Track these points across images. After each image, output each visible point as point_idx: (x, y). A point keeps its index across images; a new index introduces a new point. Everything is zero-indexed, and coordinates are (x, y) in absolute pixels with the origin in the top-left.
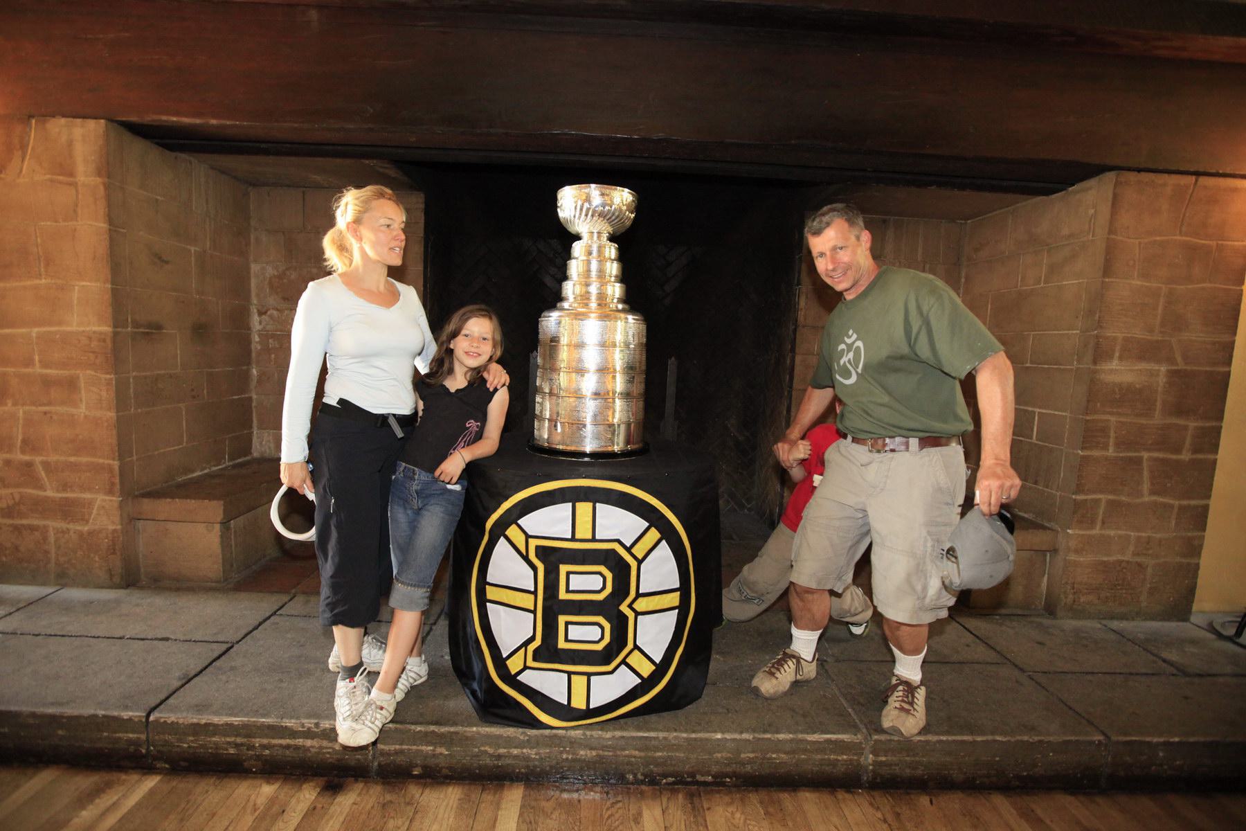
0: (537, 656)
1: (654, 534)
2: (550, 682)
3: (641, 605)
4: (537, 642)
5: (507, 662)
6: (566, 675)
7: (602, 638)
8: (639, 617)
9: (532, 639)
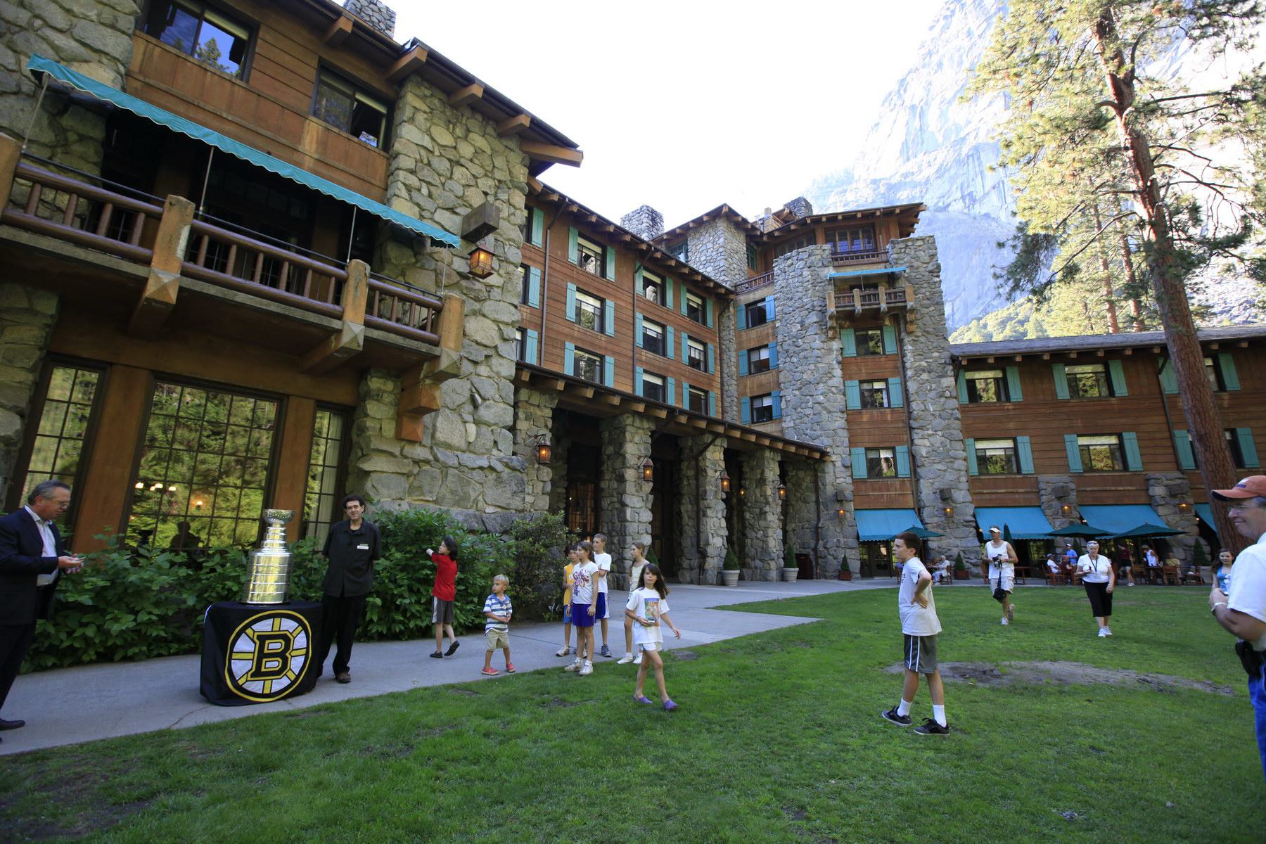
0: (252, 676)
1: (300, 628)
2: (256, 686)
3: (293, 653)
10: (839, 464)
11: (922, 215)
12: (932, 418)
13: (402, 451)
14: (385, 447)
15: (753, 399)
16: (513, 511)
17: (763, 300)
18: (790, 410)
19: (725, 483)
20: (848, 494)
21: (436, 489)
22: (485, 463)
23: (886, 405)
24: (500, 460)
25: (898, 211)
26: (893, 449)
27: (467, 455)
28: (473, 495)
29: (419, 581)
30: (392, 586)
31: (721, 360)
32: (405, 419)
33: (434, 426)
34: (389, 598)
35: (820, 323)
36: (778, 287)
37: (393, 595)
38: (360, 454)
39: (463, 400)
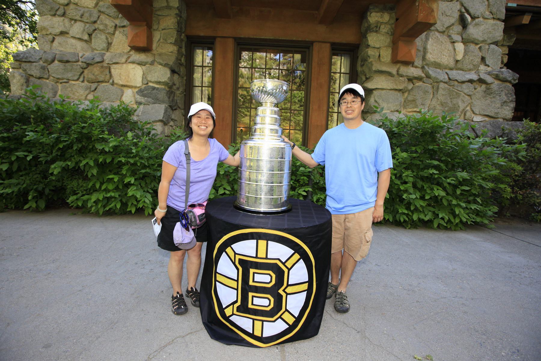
0: (238, 309)
1: (297, 256)
3: (289, 290)
4: (239, 303)
5: (225, 310)
6: (252, 320)
7: (270, 305)
8: (288, 296)
9: (236, 302)
13: (398, 71)
14: (384, 68)
16: (501, 120)
21: (428, 102)
22: (475, 77)
24: (489, 74)
27: (454, 72)
28: (462, 106)
29: (423, 179)
30: (398, 182)
32: (401, 44)
33: (425, 49)
34: (394, 191)
37: (399, 189)
38: (364, 79)
39: (452, 21)
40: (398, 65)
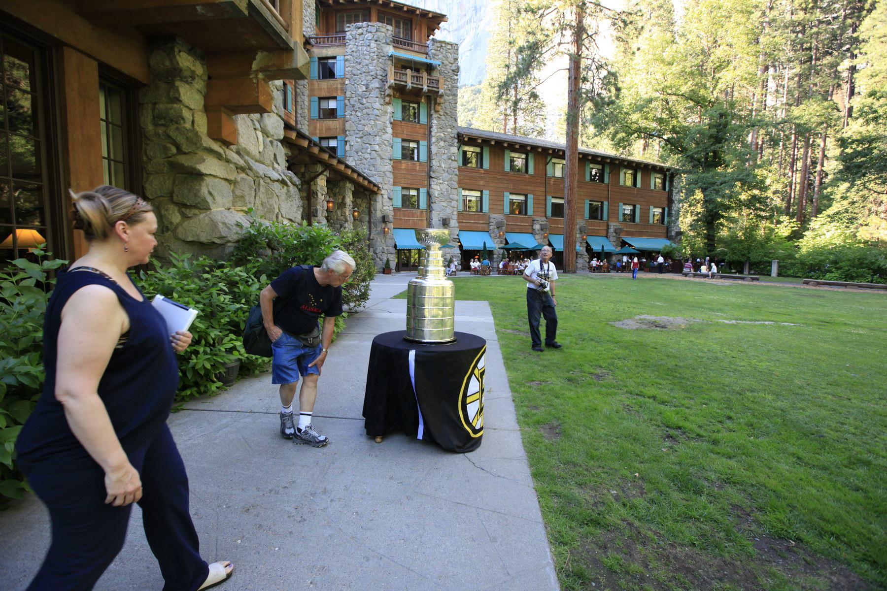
10: (385, 196)
11: (442, 24)
12: (443, 172)
15: (321, 139)
17: (335, 58)
18: (353, 153)
19: (331, 205)
20: (391, 218)
23: (416, 159)
25: (430, 15)
26: (418, 190)
31: (296, 101)
35: (381, 89)
36: (347, 50)
38: (174, 150)
40: (219, 143)
